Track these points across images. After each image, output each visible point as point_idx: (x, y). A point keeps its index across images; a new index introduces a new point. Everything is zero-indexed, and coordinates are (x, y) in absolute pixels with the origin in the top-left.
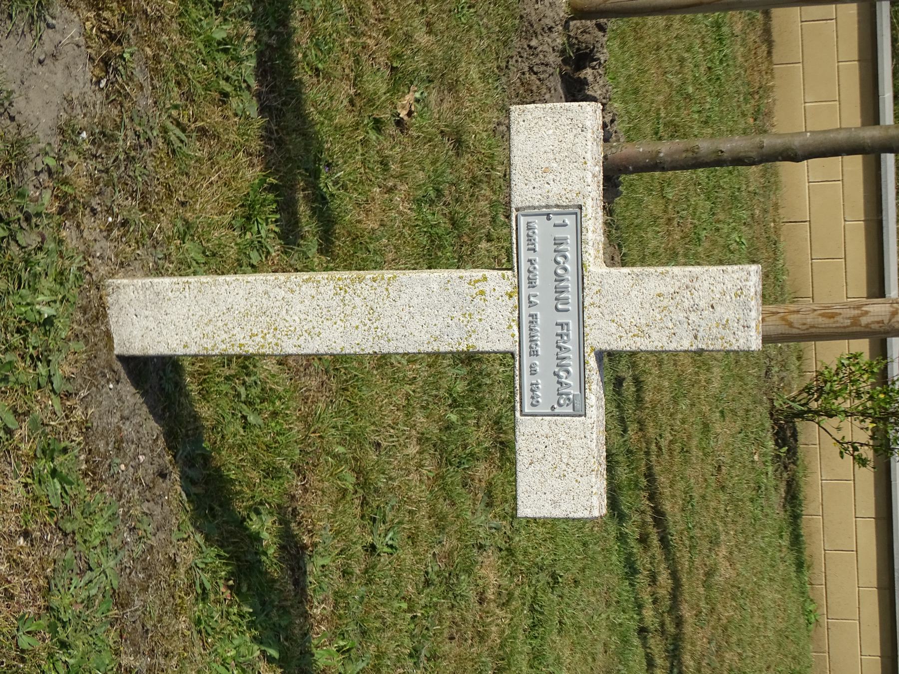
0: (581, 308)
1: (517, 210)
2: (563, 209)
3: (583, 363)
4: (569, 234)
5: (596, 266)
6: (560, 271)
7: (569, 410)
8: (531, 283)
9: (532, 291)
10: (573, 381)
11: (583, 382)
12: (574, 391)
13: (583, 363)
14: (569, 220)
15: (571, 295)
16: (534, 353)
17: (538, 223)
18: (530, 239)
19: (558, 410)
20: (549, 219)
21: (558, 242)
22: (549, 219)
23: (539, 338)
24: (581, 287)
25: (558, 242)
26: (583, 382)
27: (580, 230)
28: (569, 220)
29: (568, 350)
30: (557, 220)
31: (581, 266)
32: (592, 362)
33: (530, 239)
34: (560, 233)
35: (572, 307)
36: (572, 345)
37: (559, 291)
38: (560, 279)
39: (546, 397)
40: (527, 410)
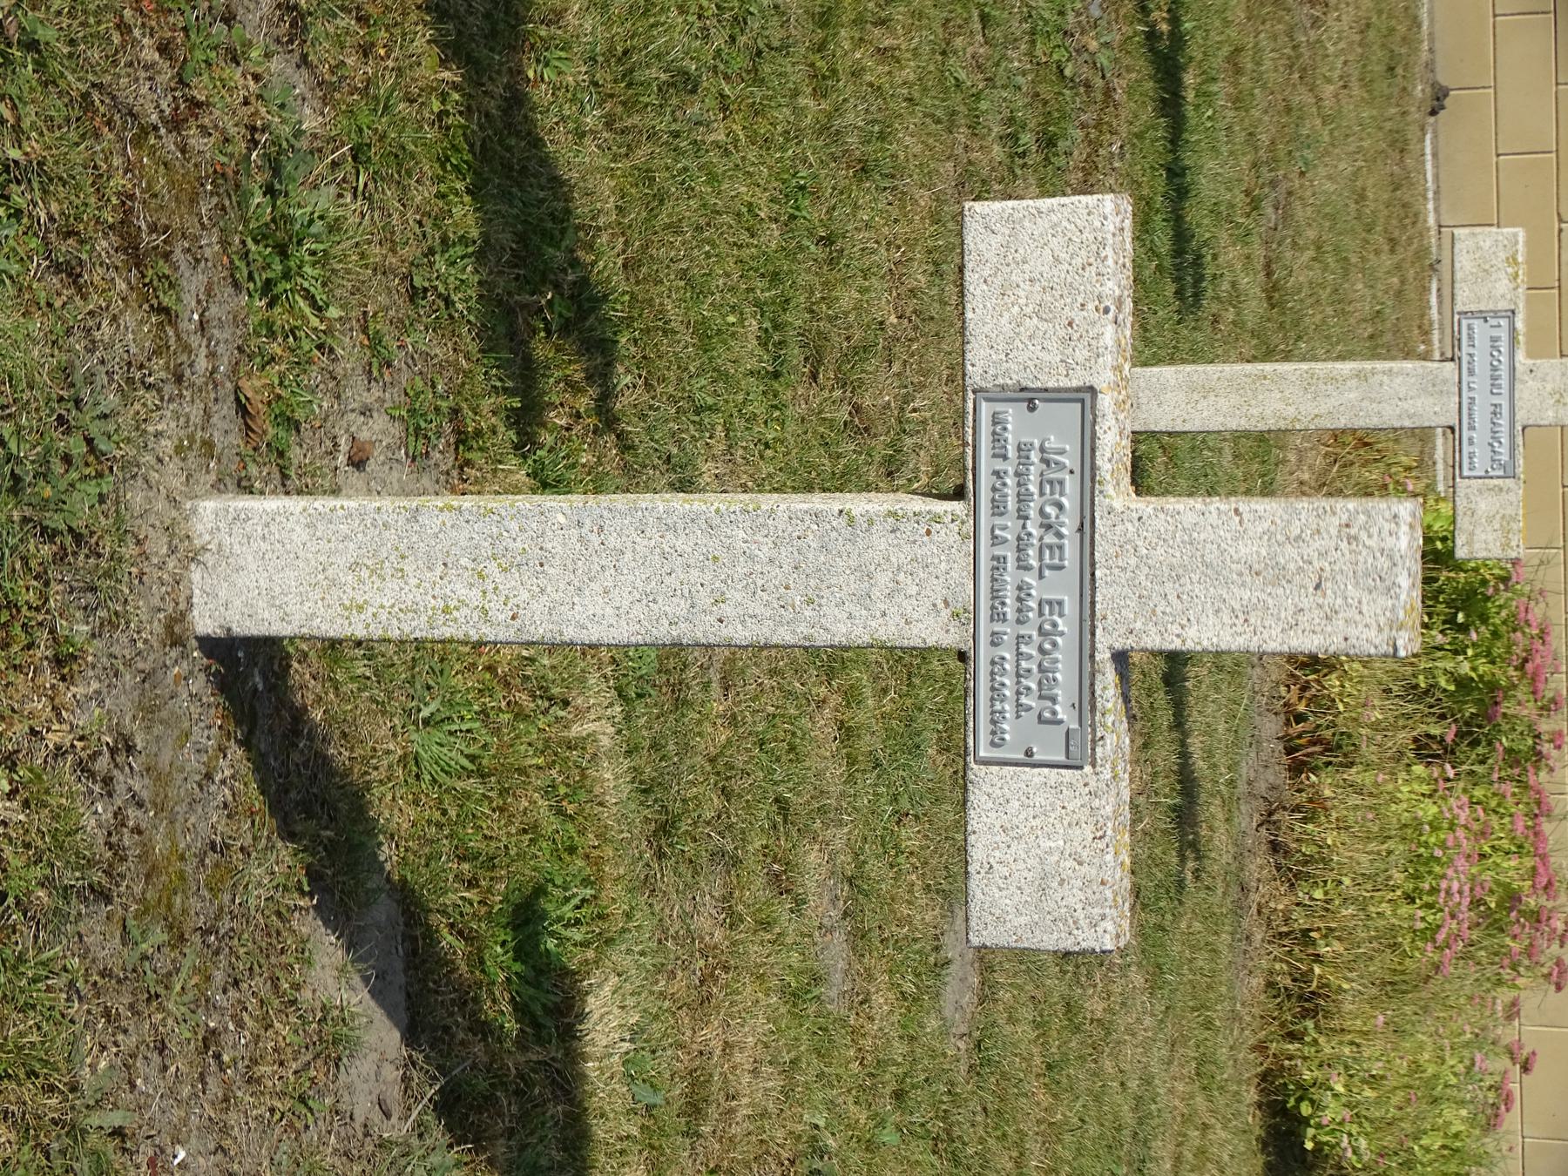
1: (1459, 313)
4: (1504, 334)
6: (1495, 363)
7: (1501, 473)
8: (1471, 372)
9: (1471, 379)
10: (1504, 451)
12: (1505, 458)
13: (1512, 437)
14: (1504, 322)
15: (1504, 382)
16: (1472, 428)
17: (1477, 324)
18: (1470, 337)
19: (1492, 473)
20: (1486, 321)
21: (1494, 340)
22: (1486, 321)
25: (1494, 340)
28: (1504, 322)
29: (1500, 425)
30: (1493, 322)
33: (1470, 337)
34: (1495, 332)
35: (1505, 391)
36: (1504, 421)
37: (1494, 378)
38: (1495, 369)
39: (1481, 463)
40: (1466, 473)
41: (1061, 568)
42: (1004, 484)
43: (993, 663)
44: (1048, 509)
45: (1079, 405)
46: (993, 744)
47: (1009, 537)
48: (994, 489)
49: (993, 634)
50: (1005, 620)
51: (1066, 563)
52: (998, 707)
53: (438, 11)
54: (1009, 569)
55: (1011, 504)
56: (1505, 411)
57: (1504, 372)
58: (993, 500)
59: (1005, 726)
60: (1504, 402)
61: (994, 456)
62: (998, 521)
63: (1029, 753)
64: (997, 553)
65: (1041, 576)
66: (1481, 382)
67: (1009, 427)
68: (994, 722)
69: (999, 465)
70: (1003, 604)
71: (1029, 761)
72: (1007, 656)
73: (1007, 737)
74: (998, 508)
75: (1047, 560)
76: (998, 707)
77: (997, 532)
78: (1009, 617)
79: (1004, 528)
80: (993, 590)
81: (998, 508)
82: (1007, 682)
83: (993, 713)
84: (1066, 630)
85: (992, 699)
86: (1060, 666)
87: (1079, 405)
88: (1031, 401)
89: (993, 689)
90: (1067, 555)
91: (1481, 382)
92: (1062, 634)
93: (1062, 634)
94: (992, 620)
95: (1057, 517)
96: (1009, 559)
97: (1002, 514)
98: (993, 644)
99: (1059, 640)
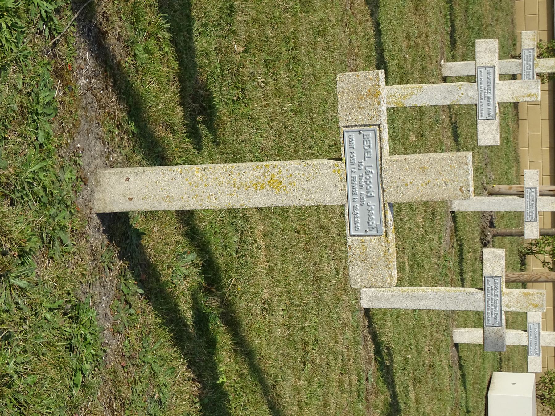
0: (539, 339)
2: (536, 324)
3: (539, 348)
4: (537, 327)
5: (542, 332)
8: (531, 335)
10: (537, 351)
11: (539, 351)
12: (538, 352)
13: (539, 348)
15: (537, 337)
23: (532, 344)
24: (539, 336)
26: (539, 351)
27: (539, 327)
28: (537, 325)
31: (539, 333)
32: (541, 348)
34: (536, 327)
35: (538, 339)
37: (536, 336)
47: (356, 171)
48: (351, 157)
56: (538, 343)
57: (537, 335)
58: (351, 160)
60: (537, 341)
62: (353, 166)
64: (353, 176)
66: (532, 337)
77: (352, 170)
79: (354, 168)
91: (532, 337)
96: (356, 177)
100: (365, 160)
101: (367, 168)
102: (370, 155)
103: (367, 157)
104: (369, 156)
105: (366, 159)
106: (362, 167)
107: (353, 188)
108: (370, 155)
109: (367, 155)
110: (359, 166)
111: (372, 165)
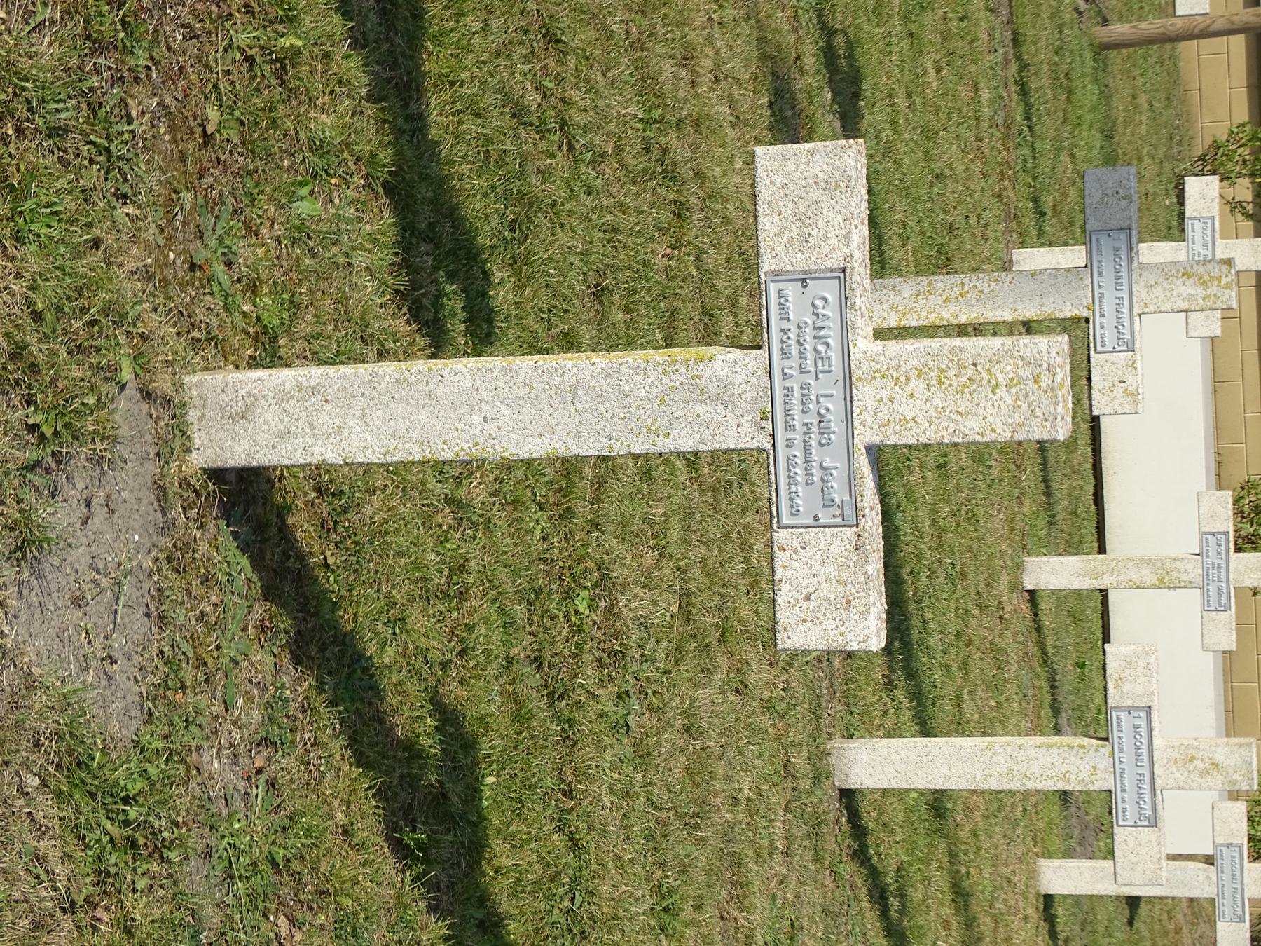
41: (830, 371)
42: (789, 338)
43: (788, 459)
44: (817, 302)
45: (837, 281)
46: (792, 514)
47: (794, 373)
49: (788, 440)
50: (795, 430)
51: (833, 368)
52: (793, 489)
53: (345, 5)
54: (796, 395)
55: (794, 351)
59: (799, 502)
61: (781, 319)
62: (786, 363)
63: (816, 518)
64: (787, 385)
65: (817, 378)
67: (790, 299)
68: (791, 499)
69: (785, 326)
70: (793, 419)
71: (816, 524)
72: (798, 454)
73: (801, 509)
74: (785, 354)
75: (820, 367)
76: (793, 489)
77: (786, 371)
78: (797, 427)
80: (786, 410)
81: (785, 354)
82: (798, 471)
83: (791, 493)
84: (836, 429)
85: (789, 484)
86: (832, 424)
87: (837, 281)
88: (804, 280)
89: (789, 477)
90: (833, 363)
92: (834, 433)
93: (834, 433)
94: (786, 430)
95: (826, 352)
96: (795, 389)
97: (788, 358)
98: (788, 446)
99: (832, 436)
100: (817, 378)
101: (822, 400)
102: (830, 366)
103: (821, 372)
104: (826, 368)
105: (820, 376)
106: (811, 406)
107: (787, 415)
108: (830, 366)
109: (823, 366)
110: (803, 403)
111: (835, 392)
